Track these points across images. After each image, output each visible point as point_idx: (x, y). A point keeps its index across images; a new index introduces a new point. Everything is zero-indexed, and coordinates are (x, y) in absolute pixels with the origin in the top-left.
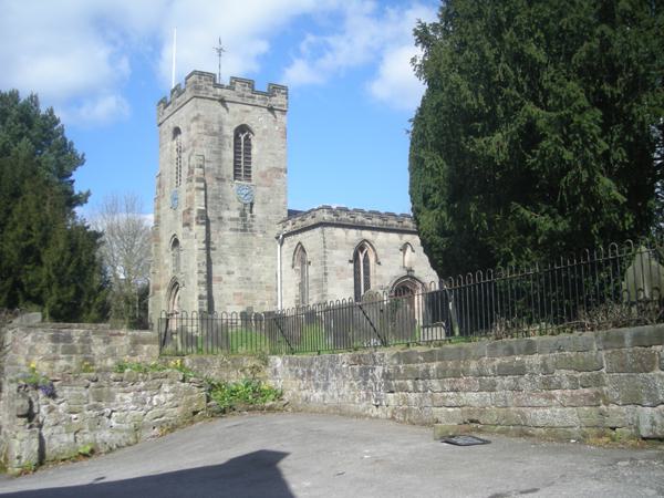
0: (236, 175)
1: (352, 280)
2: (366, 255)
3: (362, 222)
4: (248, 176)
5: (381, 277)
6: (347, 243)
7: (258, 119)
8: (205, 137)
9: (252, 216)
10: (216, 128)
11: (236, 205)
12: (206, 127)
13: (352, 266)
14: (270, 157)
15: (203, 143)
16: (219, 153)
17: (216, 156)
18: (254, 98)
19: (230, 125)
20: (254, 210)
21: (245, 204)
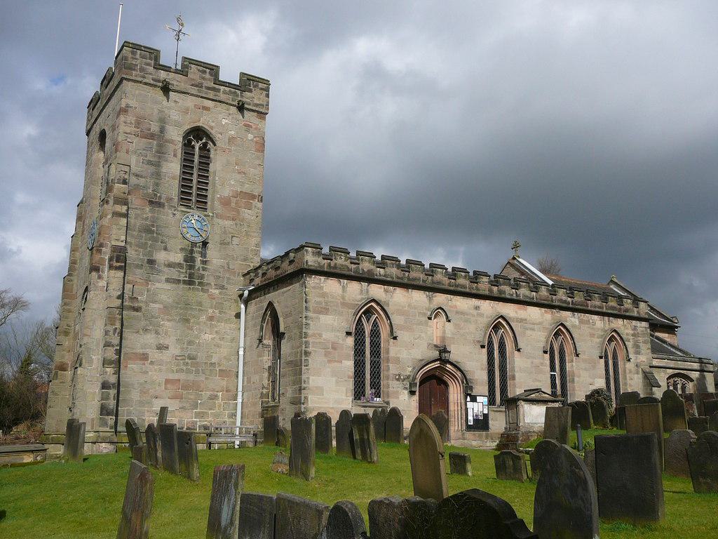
0: (185, 196)
1: (349, 364)
2: (375, 324)
3: (370, 271)
4: (202, 202)
5: (397, 360)
6: (344, 304)
7: (221, 121)
8: (136, 140)
9: (204, 262)
10: (155, 128)
11: (176, 244)
12: (138, 124)
13: (350, 341)
14: (238, 177)
15: (132, 147)
16: (157, 165)
17: (152, 169)
18: (218, 90)
19: (178, 124)
20: (209, 252)
21: (194, 244)
